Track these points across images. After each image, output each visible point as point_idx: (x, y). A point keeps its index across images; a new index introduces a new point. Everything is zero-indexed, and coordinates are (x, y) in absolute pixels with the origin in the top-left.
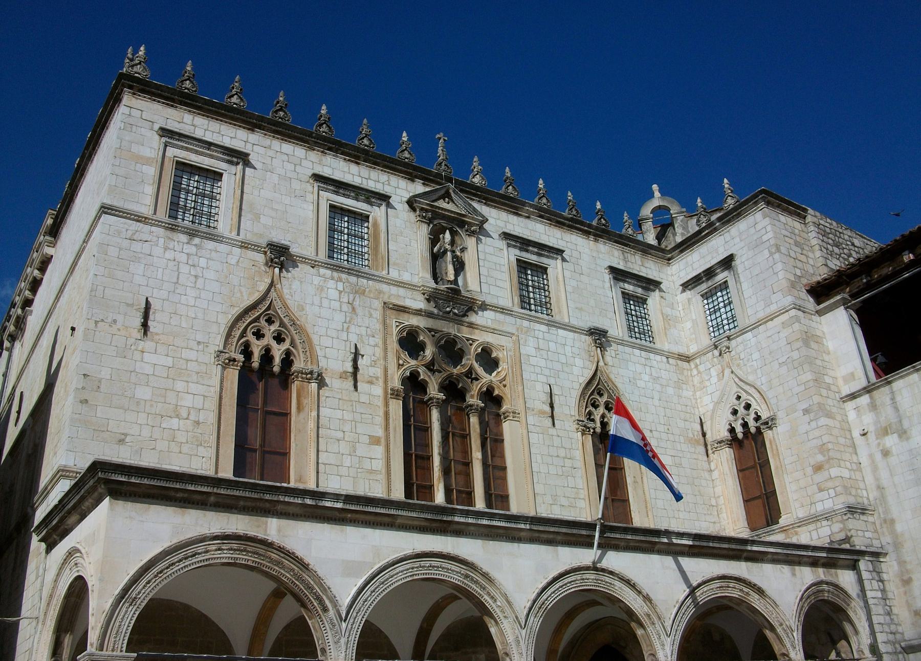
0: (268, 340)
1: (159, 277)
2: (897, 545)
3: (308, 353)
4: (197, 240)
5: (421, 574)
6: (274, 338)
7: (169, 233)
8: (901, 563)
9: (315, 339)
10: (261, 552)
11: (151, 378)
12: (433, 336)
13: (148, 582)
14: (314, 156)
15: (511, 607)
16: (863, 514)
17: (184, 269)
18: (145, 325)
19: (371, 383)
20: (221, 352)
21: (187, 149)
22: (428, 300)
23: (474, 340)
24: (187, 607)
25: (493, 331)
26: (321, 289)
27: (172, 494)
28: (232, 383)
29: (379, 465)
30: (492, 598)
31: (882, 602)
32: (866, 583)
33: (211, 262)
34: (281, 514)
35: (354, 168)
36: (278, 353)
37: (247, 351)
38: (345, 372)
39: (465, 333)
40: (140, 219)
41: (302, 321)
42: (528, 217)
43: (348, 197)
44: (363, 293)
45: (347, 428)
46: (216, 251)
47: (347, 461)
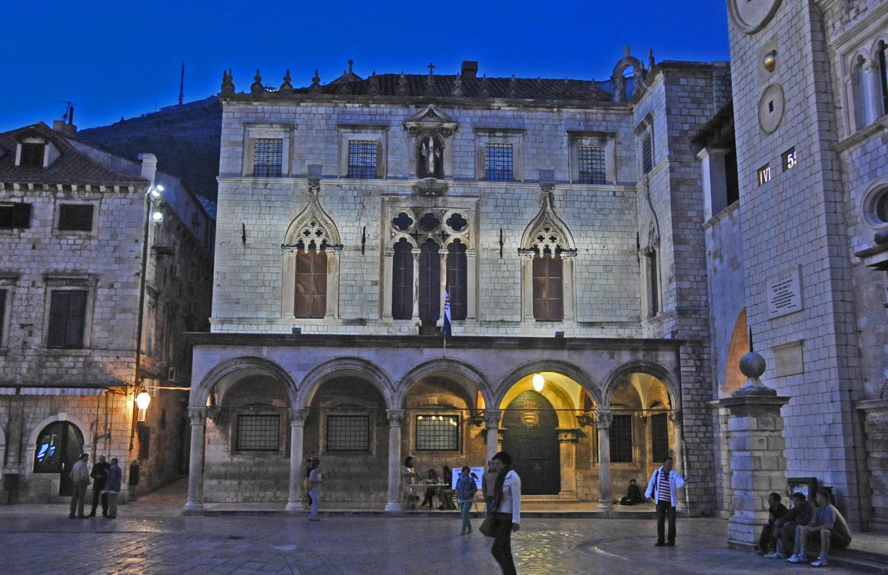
2: (715, 335)
8: (715, 348)
16: (695, 314)
18: (244, 238)
19: (373, 249)
26: (343, 198)
29: (376, 297)
31: (695, 375)
32: (682, 363)
45: (358, 279)
47: (357, 298)
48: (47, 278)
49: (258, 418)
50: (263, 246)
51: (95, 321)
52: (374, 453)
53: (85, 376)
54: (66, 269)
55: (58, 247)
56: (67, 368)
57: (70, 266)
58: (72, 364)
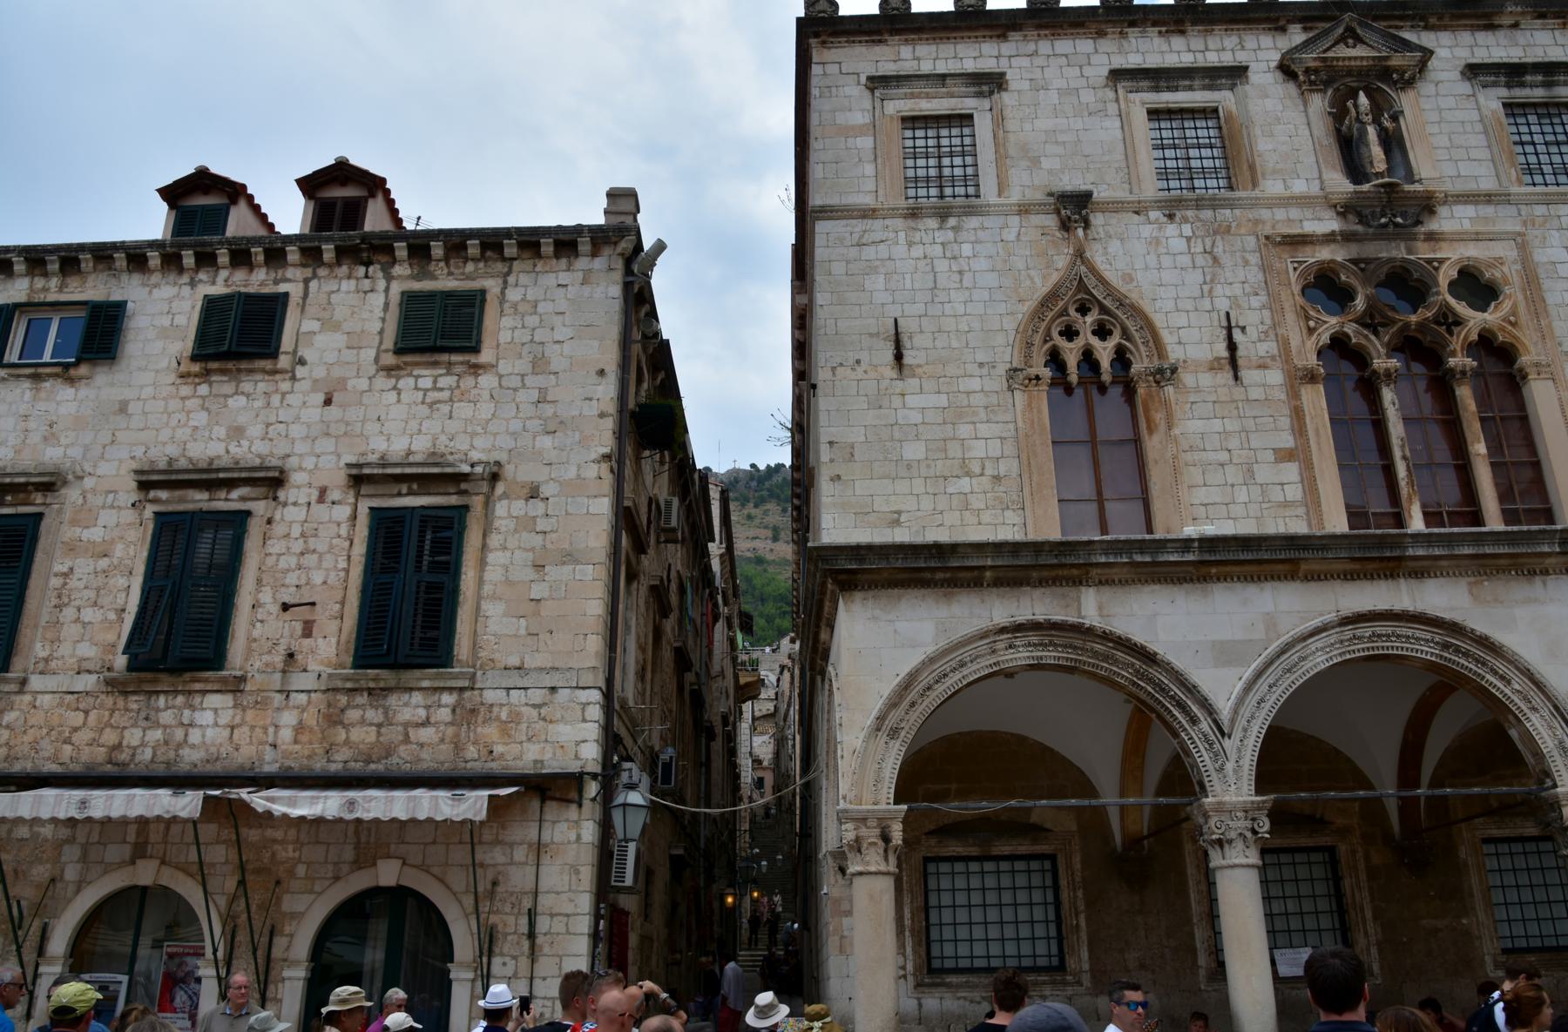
0: (1087, 337)
1: (908, 285)
3: (1151, 344)
4: (952, 221)
5: (1359, 650)
6: (1094, 333)
7: (911, 223)
9: (1159, 321)
10: (1078, 643)
11: (921, 429)
12: (1362, 270)
13: (913, 704)
14: (1106, 45)
15: (1543, 692)
17: (942, 266)
18: (899, 357)
19: (1263, 367)
20: (1016, 370)
21: (912, 96)
22: (1342, 215)
23: (1441, 261)
24: (1021, 740)
25: (1477, 238)
26: (1157, 241)
27: (928, 575)
28: (1039, 411)
30: (1502, 678)
33: (978, 247)
34: (1100, 582)
35: (1178, 42)
36: (1104, 352)
37: (1055, 360)
38: (1218, 359)
39: (1424, 252)
40: (868, 213)
41: (1134, 297)
42: (1515, 26)
43: (1176, 89)
44: (1228, 230)
45: (1234, 443)
46: (983, 228)
47: (1242, 496)
48: (359, 480)
49: (989, 866)
50: (951, 370)
51: (487, 589)
52: (1376, 968)
53: (458, 747)
54: (409, 453)
55: (393, 396)
56: (406, 725)
57: (421, 446)
58: (422, 713)
